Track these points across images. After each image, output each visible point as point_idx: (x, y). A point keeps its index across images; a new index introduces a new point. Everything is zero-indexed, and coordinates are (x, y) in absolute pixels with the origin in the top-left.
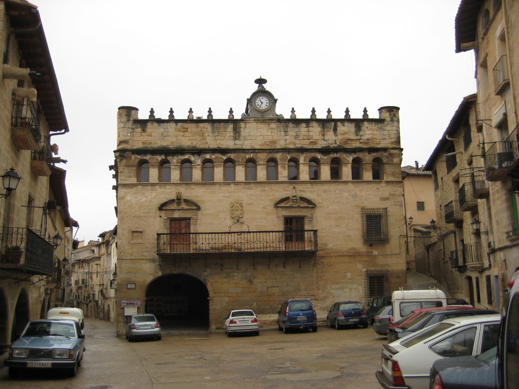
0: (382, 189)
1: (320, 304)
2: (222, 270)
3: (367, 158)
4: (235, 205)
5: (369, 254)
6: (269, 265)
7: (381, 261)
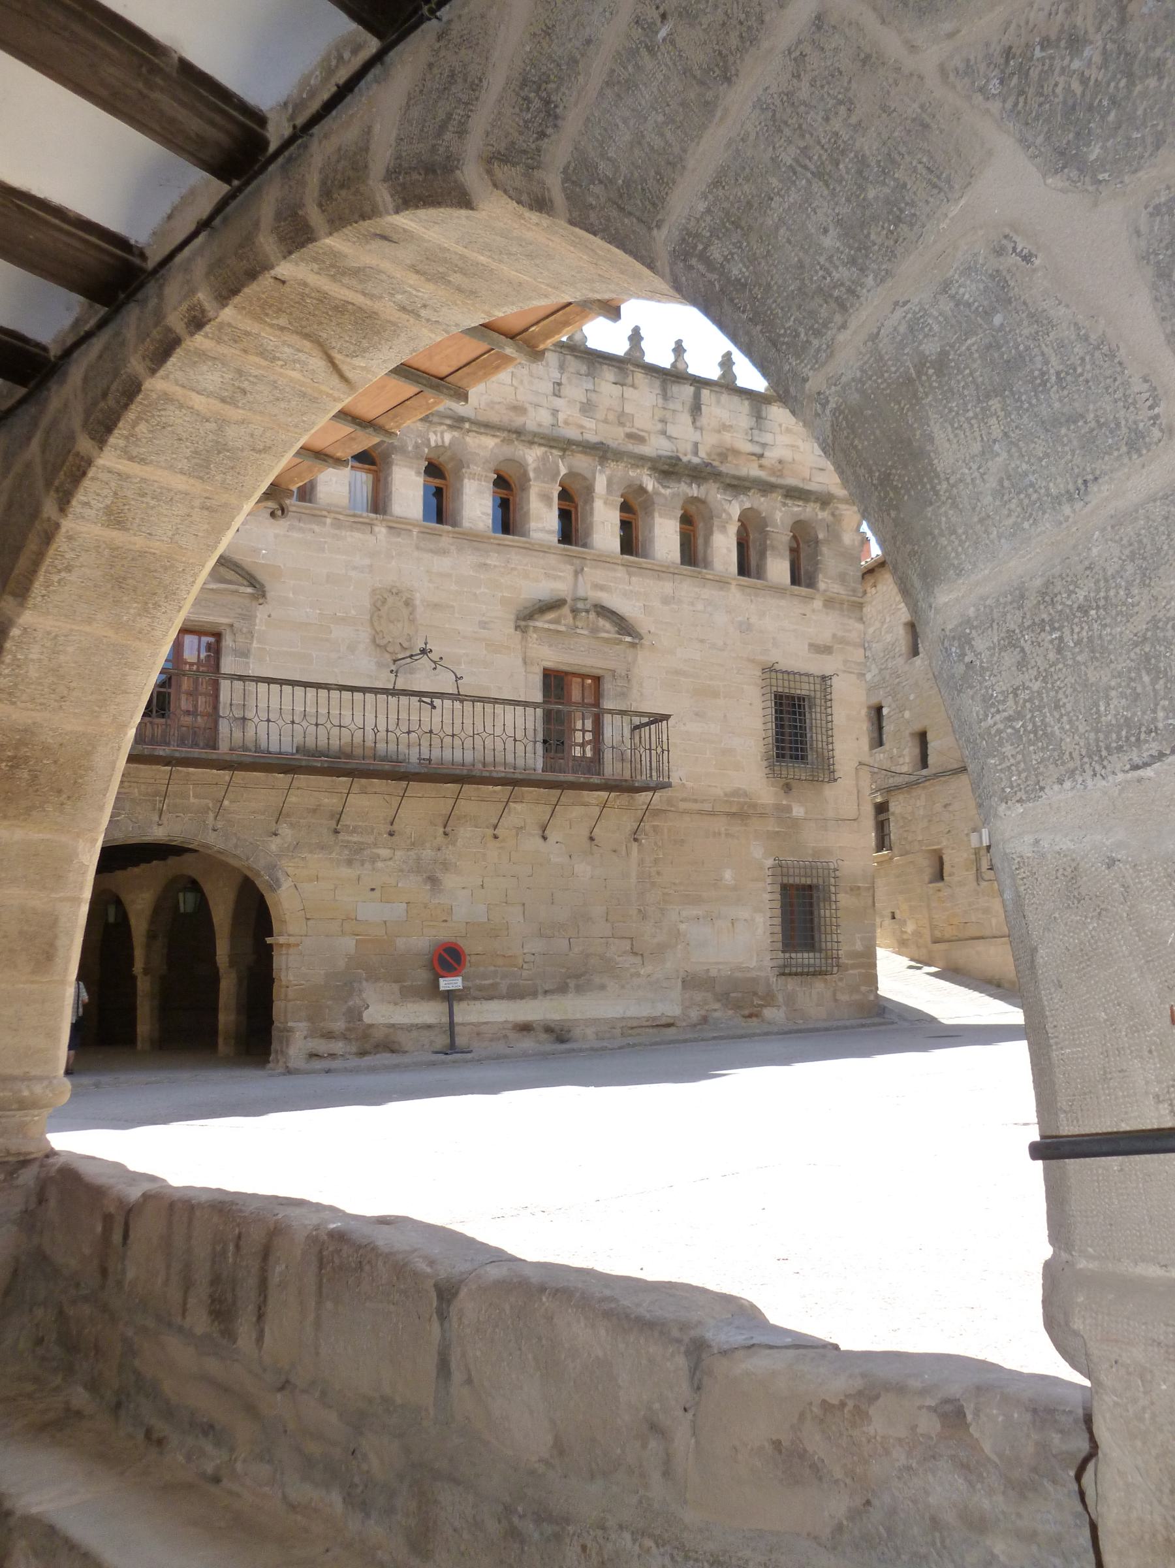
0: (814, 617)
1: (649, 969)
2: (336, 832)
3: (778, 516)
4: (391, 600)
5: (782, 811)
6: (495, 827)
7: (812, 839)
